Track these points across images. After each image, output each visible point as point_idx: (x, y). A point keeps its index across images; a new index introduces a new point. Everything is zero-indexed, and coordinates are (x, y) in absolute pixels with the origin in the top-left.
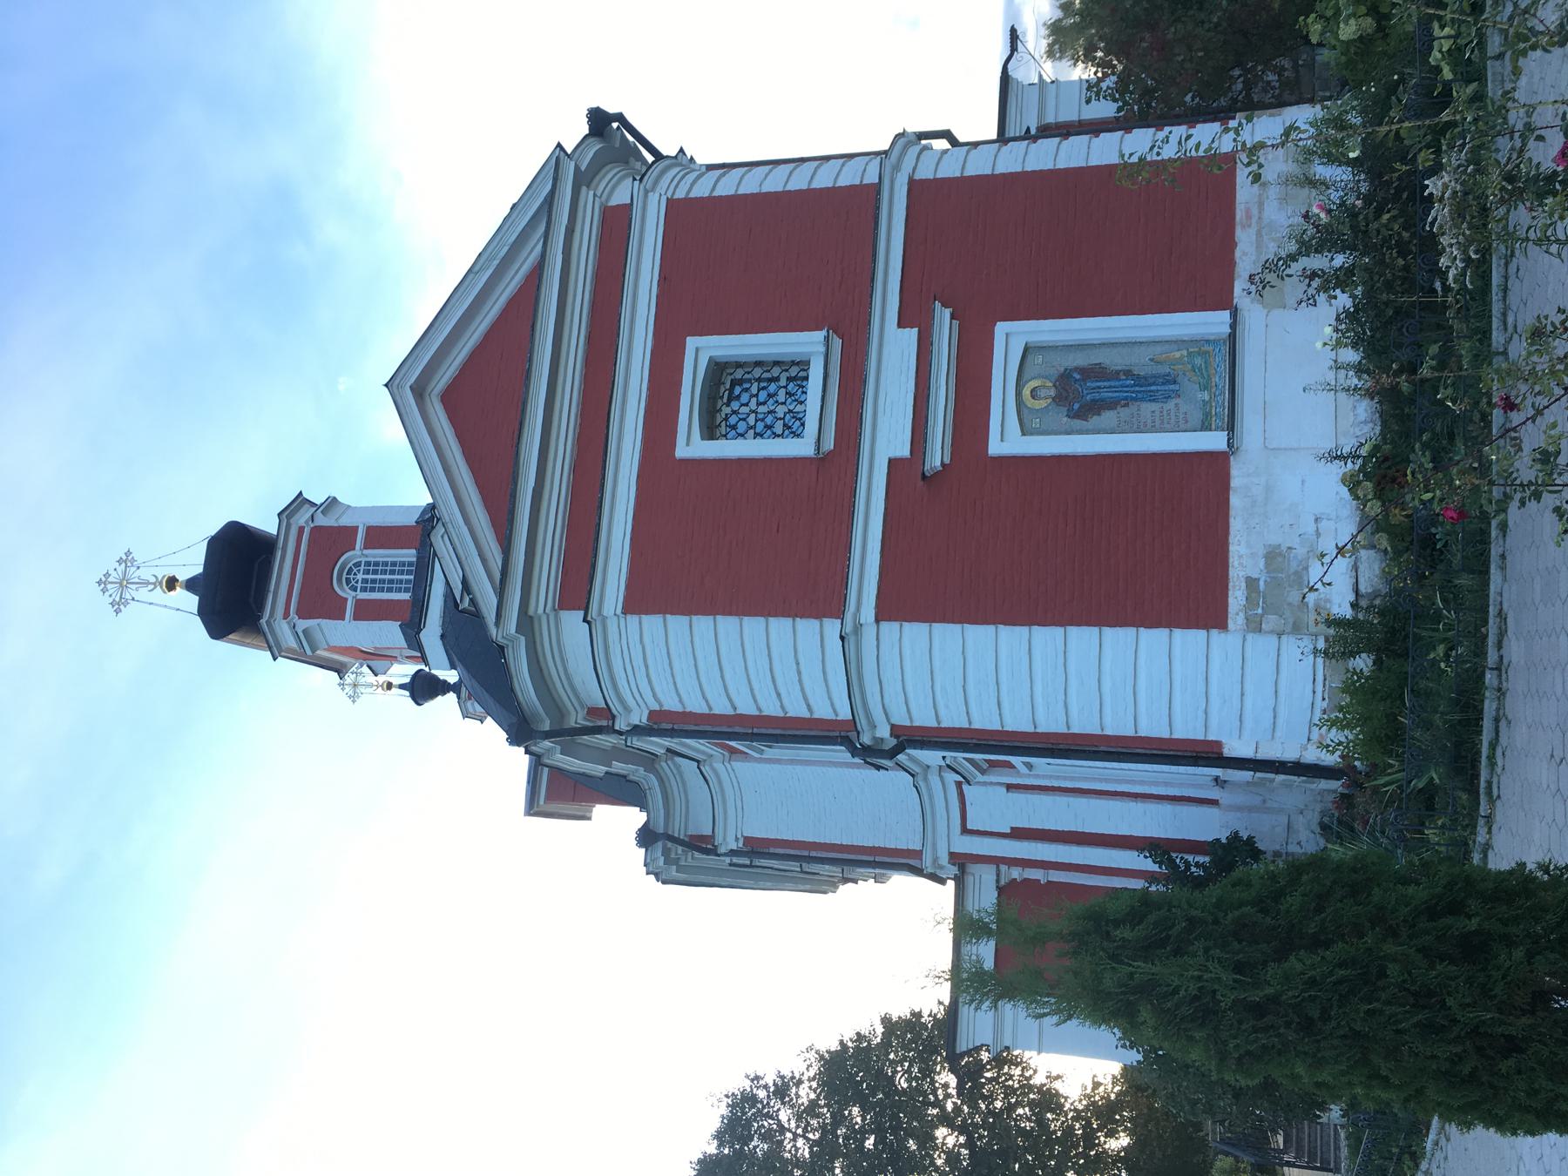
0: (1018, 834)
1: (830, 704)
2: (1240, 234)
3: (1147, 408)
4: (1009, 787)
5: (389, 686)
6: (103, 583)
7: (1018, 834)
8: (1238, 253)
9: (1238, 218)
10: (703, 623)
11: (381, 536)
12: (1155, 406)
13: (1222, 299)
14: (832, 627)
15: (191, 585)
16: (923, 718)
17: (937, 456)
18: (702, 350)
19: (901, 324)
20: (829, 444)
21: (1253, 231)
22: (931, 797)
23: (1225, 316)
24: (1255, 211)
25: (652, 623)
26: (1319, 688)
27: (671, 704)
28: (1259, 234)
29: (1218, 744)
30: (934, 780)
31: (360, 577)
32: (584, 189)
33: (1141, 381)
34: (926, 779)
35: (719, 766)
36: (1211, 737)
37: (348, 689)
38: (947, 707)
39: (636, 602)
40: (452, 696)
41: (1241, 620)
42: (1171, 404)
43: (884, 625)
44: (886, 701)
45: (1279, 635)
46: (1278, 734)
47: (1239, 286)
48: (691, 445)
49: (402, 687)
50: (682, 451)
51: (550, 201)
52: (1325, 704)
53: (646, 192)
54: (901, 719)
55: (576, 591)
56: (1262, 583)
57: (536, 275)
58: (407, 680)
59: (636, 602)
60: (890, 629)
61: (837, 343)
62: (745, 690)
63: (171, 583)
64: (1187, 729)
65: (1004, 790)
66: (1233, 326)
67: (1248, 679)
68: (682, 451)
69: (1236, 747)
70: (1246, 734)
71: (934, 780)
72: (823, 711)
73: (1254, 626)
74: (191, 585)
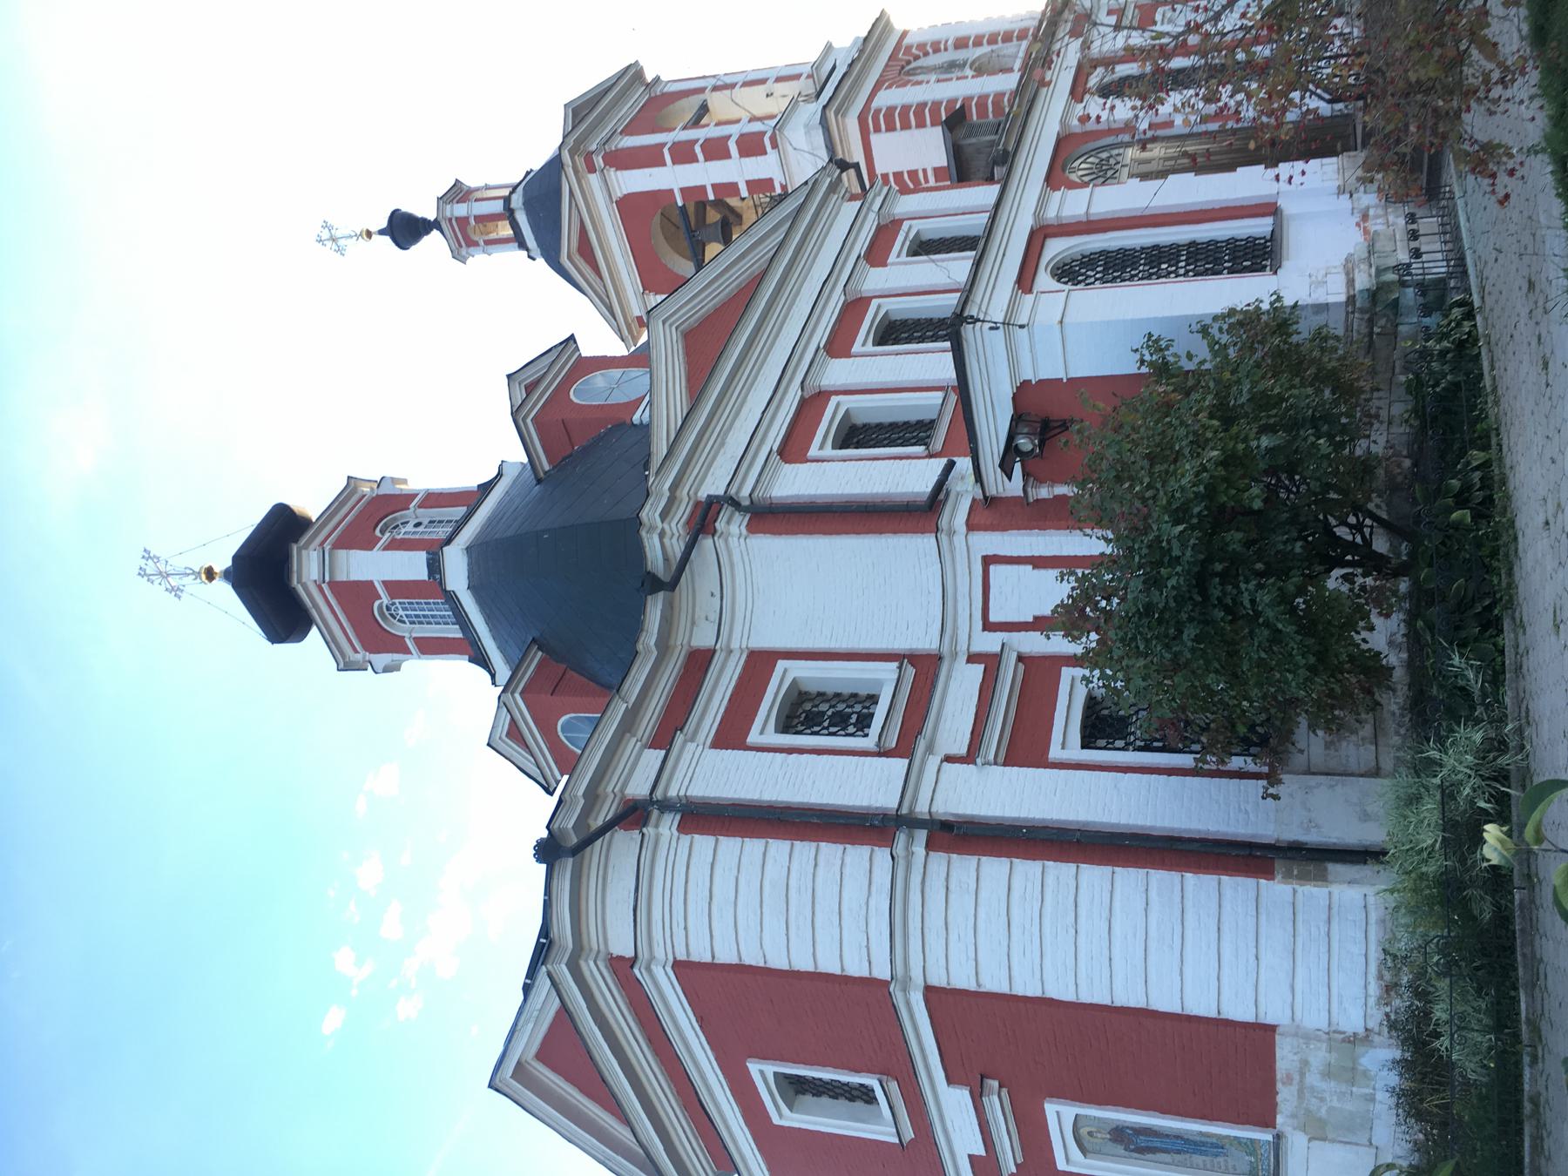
2: (1279, 1086)
3: (1198, 1159)
5: (369, 234)
6: (142, 573)
8: (1279, 1098)
9: (1279, 1076)
12: (1208, 1159)
13: (1267, 1122)
15: (227, 575)
17: (1009, 1164)
19: (950, 1081)
20: (909, 1134)
21: (1294, 1088)
24: (1297, 1077)
28: (1301, 1092)
31: (401, 612)
32: (582, 963)
33: (1187, 1141)
37: (329, 244)
40: (435, 233)
42: (1221, 1159)
47: (1279, 1119)
49: (381, 232)
53: (648, 969)
58: (384, 224)
61: (893, 1086)
63: (210, 574)
74: (227, 575)
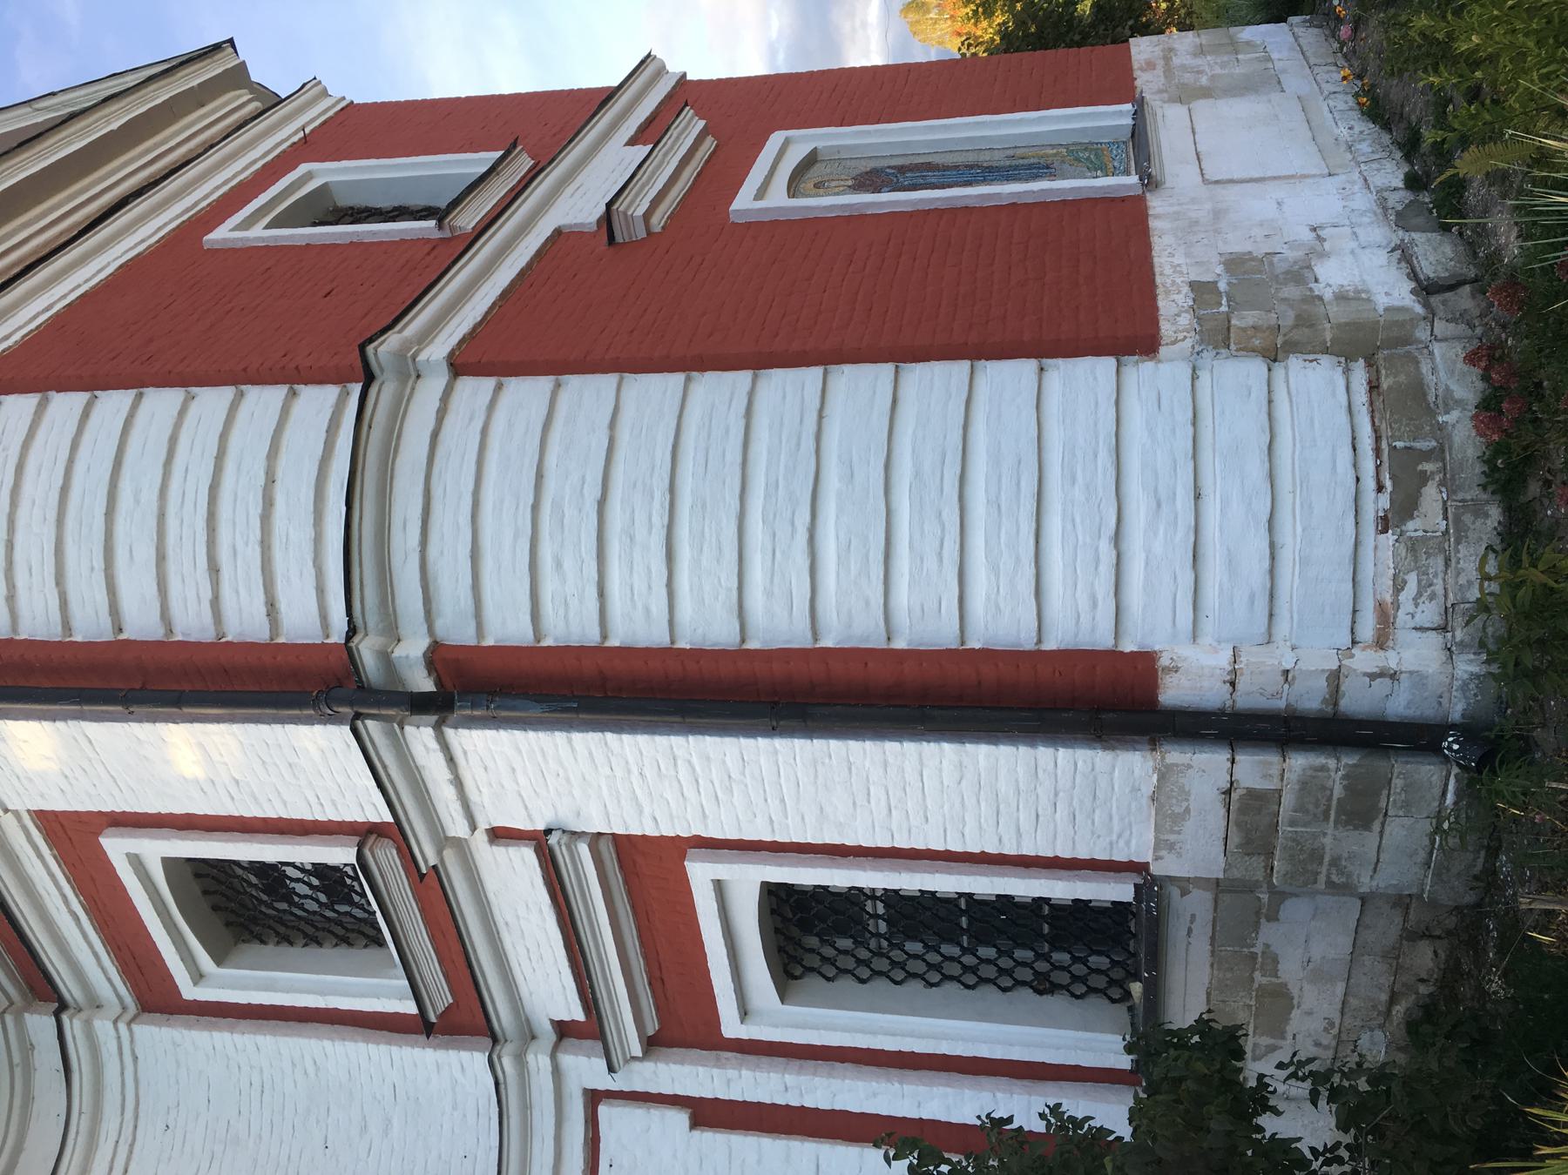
16: (507, 626)
22: (526, 1107)
23: (1128, 107)
26: (1368, 465)
29: (1144, 666)
30: (539, 1061)
34: (520, 1059)
35: (103, 1027)
36: (1128, 646)
38: (559, 564)
41: (1185, 320)
43: (467, 384)
44: (432, 552)
45: (1273, 356)
46: (1283, 628)
52: (1385, 501)
54: (458, 630)
56: (1222, 286)
62: (146, 553)
64: (1076, 619)
65: (681, 1118)
66: (1139, 115)
67: (1206, 455)
69: (1193, 678)
70: (1208, 627)
71: (539, 1061)
73: (1217, 337)
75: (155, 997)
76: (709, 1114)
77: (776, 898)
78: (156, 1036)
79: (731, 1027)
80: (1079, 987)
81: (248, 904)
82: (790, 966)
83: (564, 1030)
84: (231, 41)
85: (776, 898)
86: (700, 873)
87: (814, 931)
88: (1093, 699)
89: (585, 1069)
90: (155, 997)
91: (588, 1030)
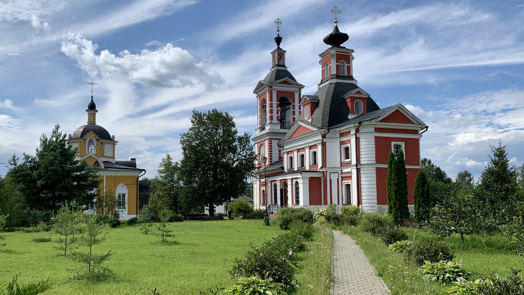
0: (331, 180)
1: (363, 161)
4: (338, 180)
7: (331, 180)
10: (374, 146)
11: (349, 69)
14: (374, 162)
18: (403, 144)
25: (374, 139)
27: (361, 140)
39: (376, 137)
48: (393, 143)
50: (392, 142)
51: (420, 124)
55: (377, 130)
57: (414, 124)
59: (376, 137)
60: (375, 169)
68: (392, 142)
72: (362, 160)
75: (342, 143)
76: (338, 180)
77: (349, 185)
78: (339, 143)
79: (343, 181)
80: (347, 202)
81: (347, 149)
82: (347, 185)
83: (342, 171)
84: (427, 127)
85: (349, 185)
86: (350, 181)
87: (348, 186)
88: (359, 202)
89: (340, 172)
90: (342, 143)
91: (342, 173)
